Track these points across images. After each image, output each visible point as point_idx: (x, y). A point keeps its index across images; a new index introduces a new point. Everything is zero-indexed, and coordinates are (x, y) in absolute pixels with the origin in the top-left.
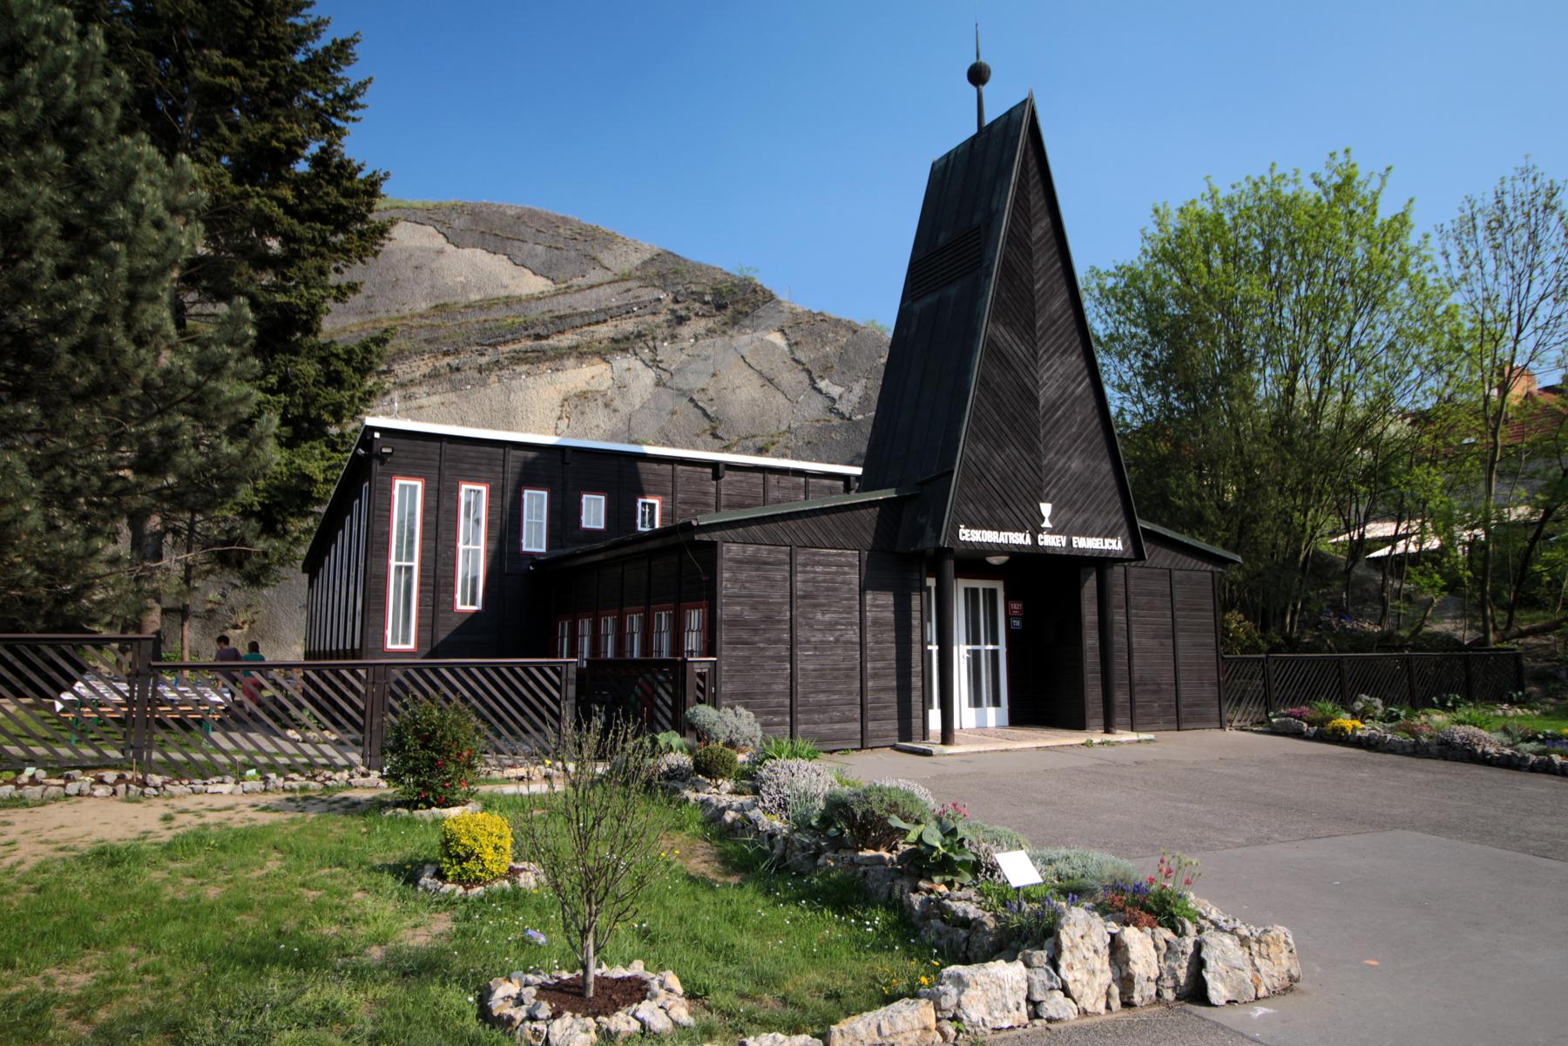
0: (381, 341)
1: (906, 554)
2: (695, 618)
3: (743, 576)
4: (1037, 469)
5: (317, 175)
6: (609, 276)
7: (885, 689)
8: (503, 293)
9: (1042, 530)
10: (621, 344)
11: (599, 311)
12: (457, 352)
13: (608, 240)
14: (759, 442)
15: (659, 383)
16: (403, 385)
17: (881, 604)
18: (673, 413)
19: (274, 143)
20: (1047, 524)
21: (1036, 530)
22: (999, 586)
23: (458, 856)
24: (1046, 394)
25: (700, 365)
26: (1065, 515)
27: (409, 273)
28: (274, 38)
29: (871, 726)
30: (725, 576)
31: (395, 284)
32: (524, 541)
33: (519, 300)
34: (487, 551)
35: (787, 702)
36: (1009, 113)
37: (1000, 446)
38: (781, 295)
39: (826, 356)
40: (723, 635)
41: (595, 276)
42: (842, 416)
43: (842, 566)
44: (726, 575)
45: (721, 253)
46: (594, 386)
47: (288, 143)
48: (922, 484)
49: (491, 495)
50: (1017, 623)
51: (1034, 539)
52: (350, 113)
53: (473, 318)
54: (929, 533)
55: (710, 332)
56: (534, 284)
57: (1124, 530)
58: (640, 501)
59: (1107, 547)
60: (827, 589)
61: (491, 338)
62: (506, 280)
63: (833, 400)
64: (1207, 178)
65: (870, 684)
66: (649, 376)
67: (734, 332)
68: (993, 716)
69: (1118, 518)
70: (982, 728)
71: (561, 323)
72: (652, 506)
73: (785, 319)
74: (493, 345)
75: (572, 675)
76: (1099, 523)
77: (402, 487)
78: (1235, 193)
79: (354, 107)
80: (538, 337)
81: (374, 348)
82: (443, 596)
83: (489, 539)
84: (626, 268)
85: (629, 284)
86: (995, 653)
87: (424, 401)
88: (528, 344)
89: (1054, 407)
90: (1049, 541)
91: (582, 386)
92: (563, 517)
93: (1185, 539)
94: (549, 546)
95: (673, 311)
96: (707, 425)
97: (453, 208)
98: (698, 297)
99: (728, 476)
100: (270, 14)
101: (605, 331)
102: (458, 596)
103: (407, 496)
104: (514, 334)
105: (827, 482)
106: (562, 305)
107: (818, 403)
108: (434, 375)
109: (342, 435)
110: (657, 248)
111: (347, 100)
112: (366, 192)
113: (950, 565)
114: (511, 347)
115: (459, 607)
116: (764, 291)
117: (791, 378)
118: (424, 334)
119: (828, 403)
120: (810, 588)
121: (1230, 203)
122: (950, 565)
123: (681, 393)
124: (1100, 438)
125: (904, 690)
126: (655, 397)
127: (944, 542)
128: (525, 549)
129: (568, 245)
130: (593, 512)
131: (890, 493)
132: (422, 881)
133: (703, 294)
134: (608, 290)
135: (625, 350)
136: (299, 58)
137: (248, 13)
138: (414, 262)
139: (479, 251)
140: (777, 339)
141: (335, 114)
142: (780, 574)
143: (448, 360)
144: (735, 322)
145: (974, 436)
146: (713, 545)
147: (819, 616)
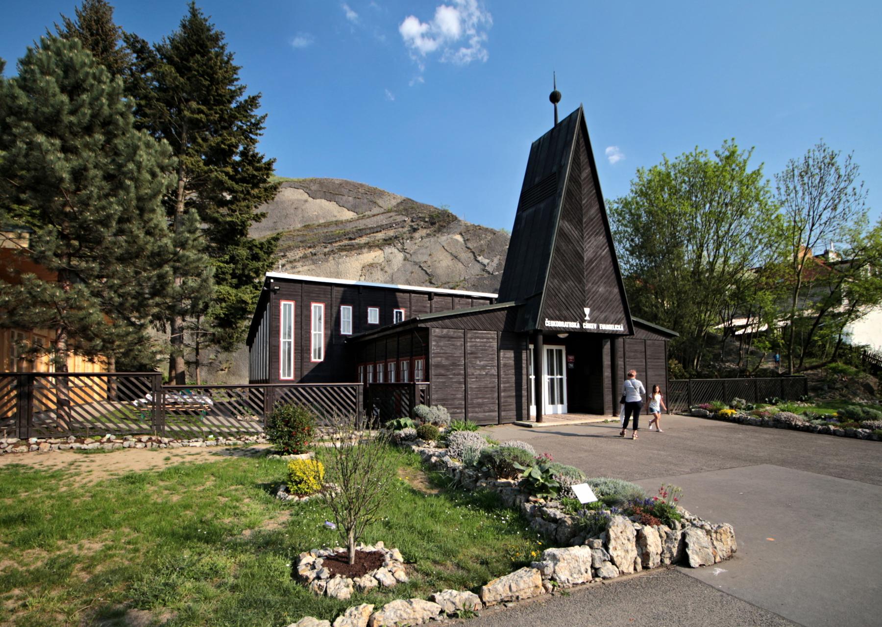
0: (276, 239)
1: (519, 332)
2: (420, 364)
3: (442, 344)
4: (583, 291)
5: (243, 161)
6: (382, 210)
7: (509, 397)
8: (334, 219)
9: (585, 321)
10: (388, 242)
11: (378, 227)
12: (314, 247)
13: (381, 194)
14: (451, 285)
15: (405, 259)
16: (291, 262)
17: (508, 356)
18: (412, 273)
19: (223, 146)
20: (587, 318)
21: (582, 321)
22: (563, 348)
23: (295, 481)
24: (587, 255)
25: (424, 251)
26: (596, 314)
27: (292, 211)
28: (220, 95)
29: (503, 414)
30: (433, 344)
31: (286, 216)
32: (342, 329)
33: (342, 222)
34: (326, 335)
35: (463, 403)
36: (571, 115)
37: (565, 281)
38: (460, 218)
39: (481, 246)
40: (433, 372)
41: (376, 210)
42: (488, 273)
43: (490, 338)
44: (434, 343)
45: (433, 199)
46: (376, 261)
47: (229, 146)
48: (527, 299)
49: (326, 308)
50: (571, 365)
51: (581, 325)
52: (258, 132)
53: (322, 231)
54: (531, 323)
55: (428, 235)
56: (349, 215)
57: (624, 321)
58: (395, 311)
59: (616, 329)
60: (482, 350)
61: (329, 240)
62: (336, 214)
63: (485, 265)
64: (663, 155)
65: (502, 394)
66: (400, 256)
67: (439, 235)
68: (561, 408)
69: (621, 315)
70: (555, 415)
71: (361, 232)
72: (400, 313)
73: (462, 229)
74: (330, 243)
75: (361, 391)
76: (612, 317)
77: (285, 305)
78: (677, 161)
79: (260, 129)
80: (351, 239)
81: (273, 242)
82: (305, 355)
83: (326, 328)
84: (390, 206)
85: (391, 214)
86: (561, 380)
87: (300, 269)
88: (347, 242)
89: (591, 261)
90: (588, 326)
91: (371, 261)
92: (359, 318)
93: (653, 325)
94: (354, 331)
95: (411, 226)
96: (427, 278)
97: (311, 181)
98: (423, 219)
99: (436, 299)
100: (218, 84)
101: (380, 236)
102: (312, 355)
103: (287, 309)
104: (339, 238)
105: (482, 301)
106: (361, 224)
107: (478, 267)
108: (305, 257)
109: (260, 283)
110: (404, 196)
111: (257, 125)
112: (266, 168)
113: (541, 338)
115: (313, 360)
116: (453, 216)
117: (465, 256)
118: (300, 239)
119: (482, 267)
120: (474, 349)
121: (674, 166)
122: (541, 338)
123: (416, 263)
124: (614, 276)
125: (519, 397)
126: (404, 265)
127: (538, 327)
128: (342, 333)
129: (363, 196)
130: (373, 316)
131: (512, 304)
132: (279, 493)
133: (424, 218)
134: (382, 217)
135: (390, 244)
136: (233, 105)
137: (207, 83)
138: (294, 206)
139: (323, 200)
140: (459, 238)
141: (251, 132)
142: (459, 343)
143: (310, 250)
144: (439, 230)
145: (553, 276)
146: (427, 329)
147: (478, 363)
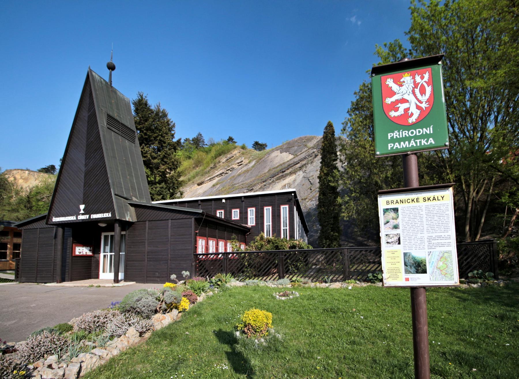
10: (301, 168)
12: (266, 181)
80: (283, 172)
88: (281, 174)
101: (298, 165)
114: (277, 176)
